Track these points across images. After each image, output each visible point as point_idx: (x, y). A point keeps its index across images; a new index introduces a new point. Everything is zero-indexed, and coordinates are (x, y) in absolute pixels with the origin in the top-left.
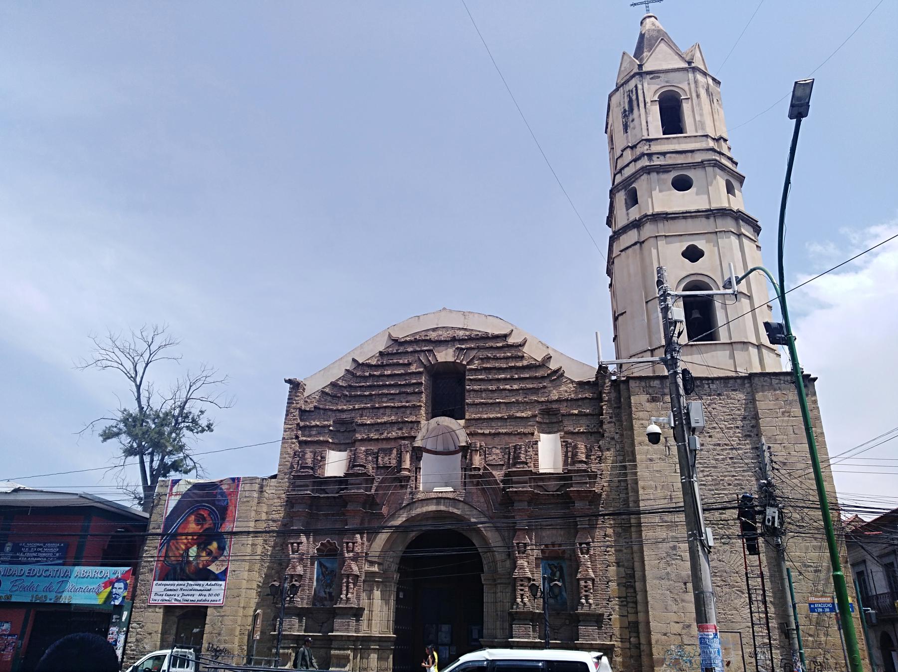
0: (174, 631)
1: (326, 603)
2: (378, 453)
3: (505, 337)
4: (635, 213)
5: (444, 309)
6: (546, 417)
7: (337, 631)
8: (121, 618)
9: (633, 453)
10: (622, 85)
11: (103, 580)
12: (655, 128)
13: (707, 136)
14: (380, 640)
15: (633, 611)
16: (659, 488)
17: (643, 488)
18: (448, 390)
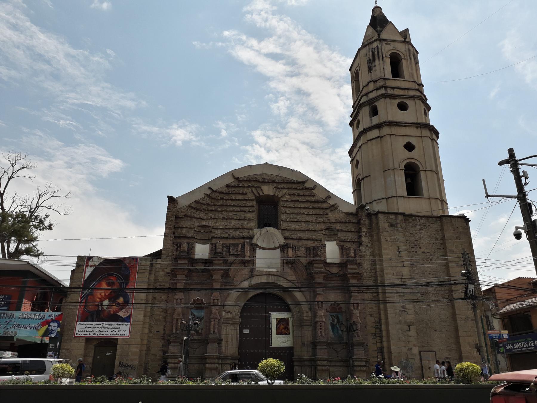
0: (92, 354)
1: (195, 337)
2: (229, 246)
3: (304, 183)
4: (376, 120)
5: (266, 163)
6: (327, 231)
7: (209, 353)
8: (56, 346)
9: (380, 255)
10: (368, 44)
11: (42, 321)
12: (388, 74)
13: (415, 82)
14: (232, 359)
15: (379, 341)
16: (395, 274)
17: (387, 274)
18: (268, 212)
